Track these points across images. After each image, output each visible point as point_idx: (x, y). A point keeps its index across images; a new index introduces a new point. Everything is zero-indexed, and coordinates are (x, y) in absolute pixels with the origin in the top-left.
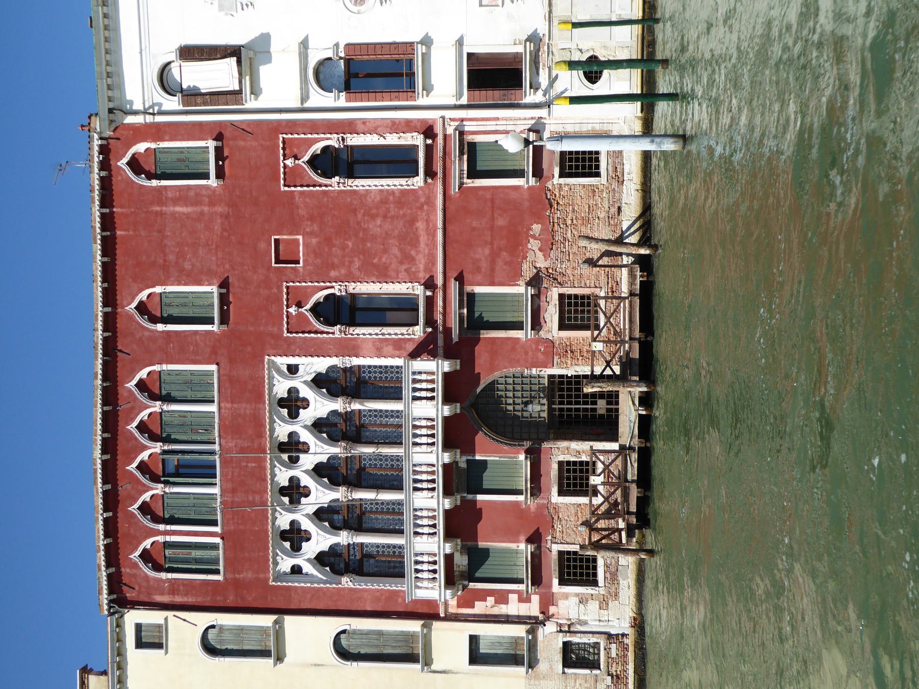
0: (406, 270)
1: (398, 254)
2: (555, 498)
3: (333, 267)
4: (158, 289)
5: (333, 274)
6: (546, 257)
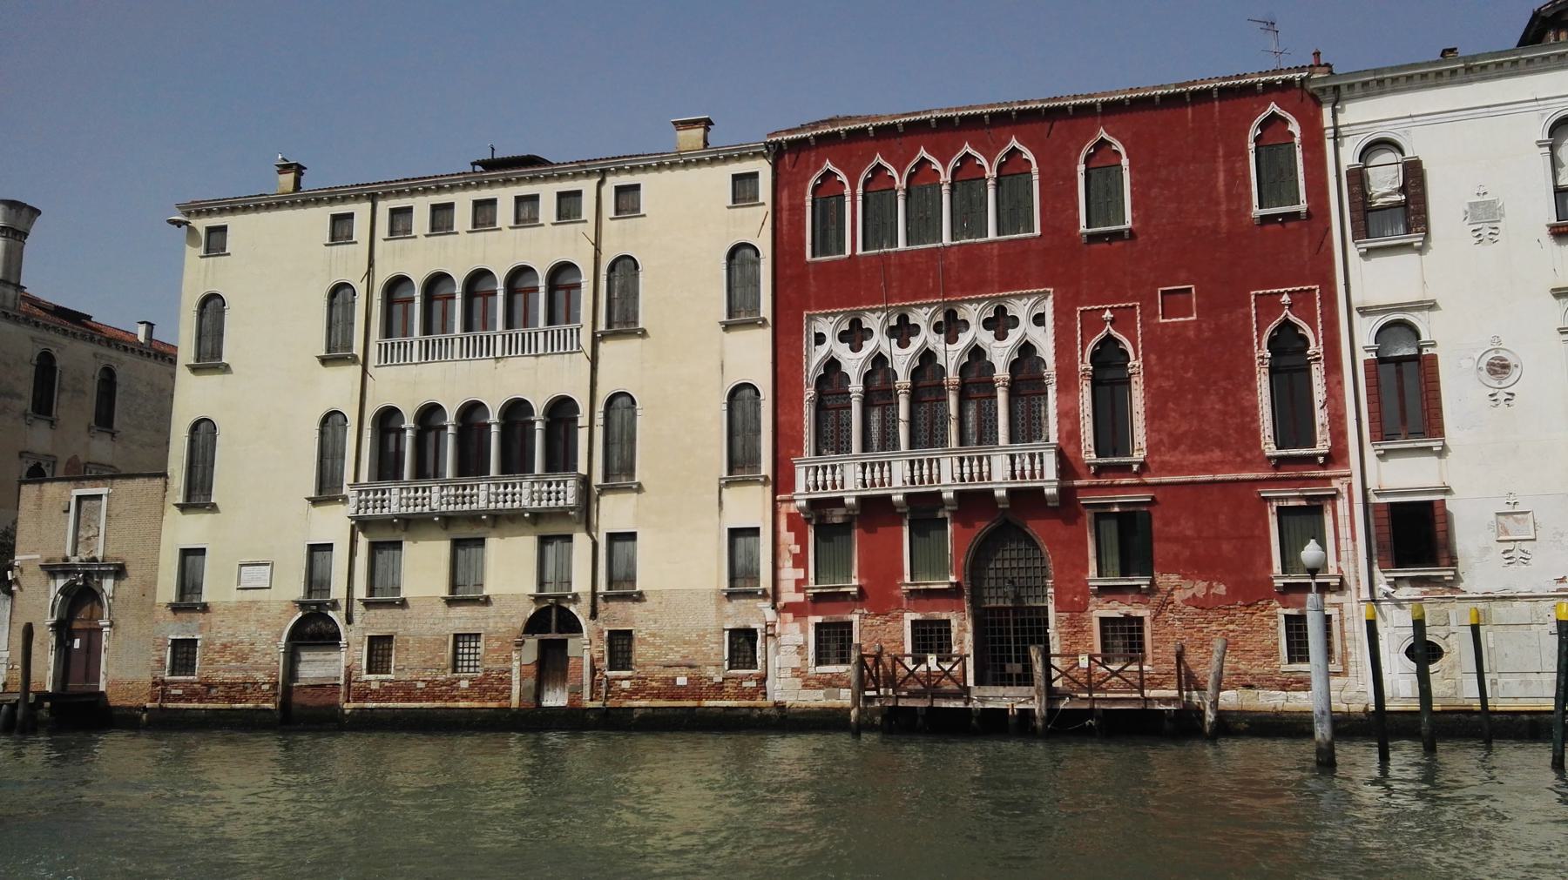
0: (1161, 441)
1: (1180, 431)
2: (909, 617)
3: (1161, 358)
4: (1125, 162)
5: (1153, 357)
6: (1187, 602)
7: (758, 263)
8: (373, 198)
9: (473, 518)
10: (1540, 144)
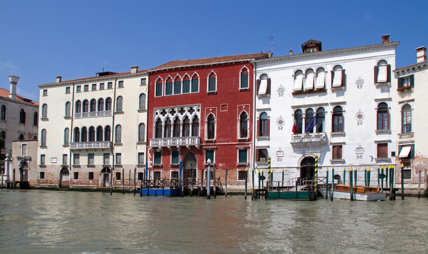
2: (171, 171)
4: (216, 77)
7: (145, 97)
8: (74, 84)
9: (92, 150)
10: (293, 76)
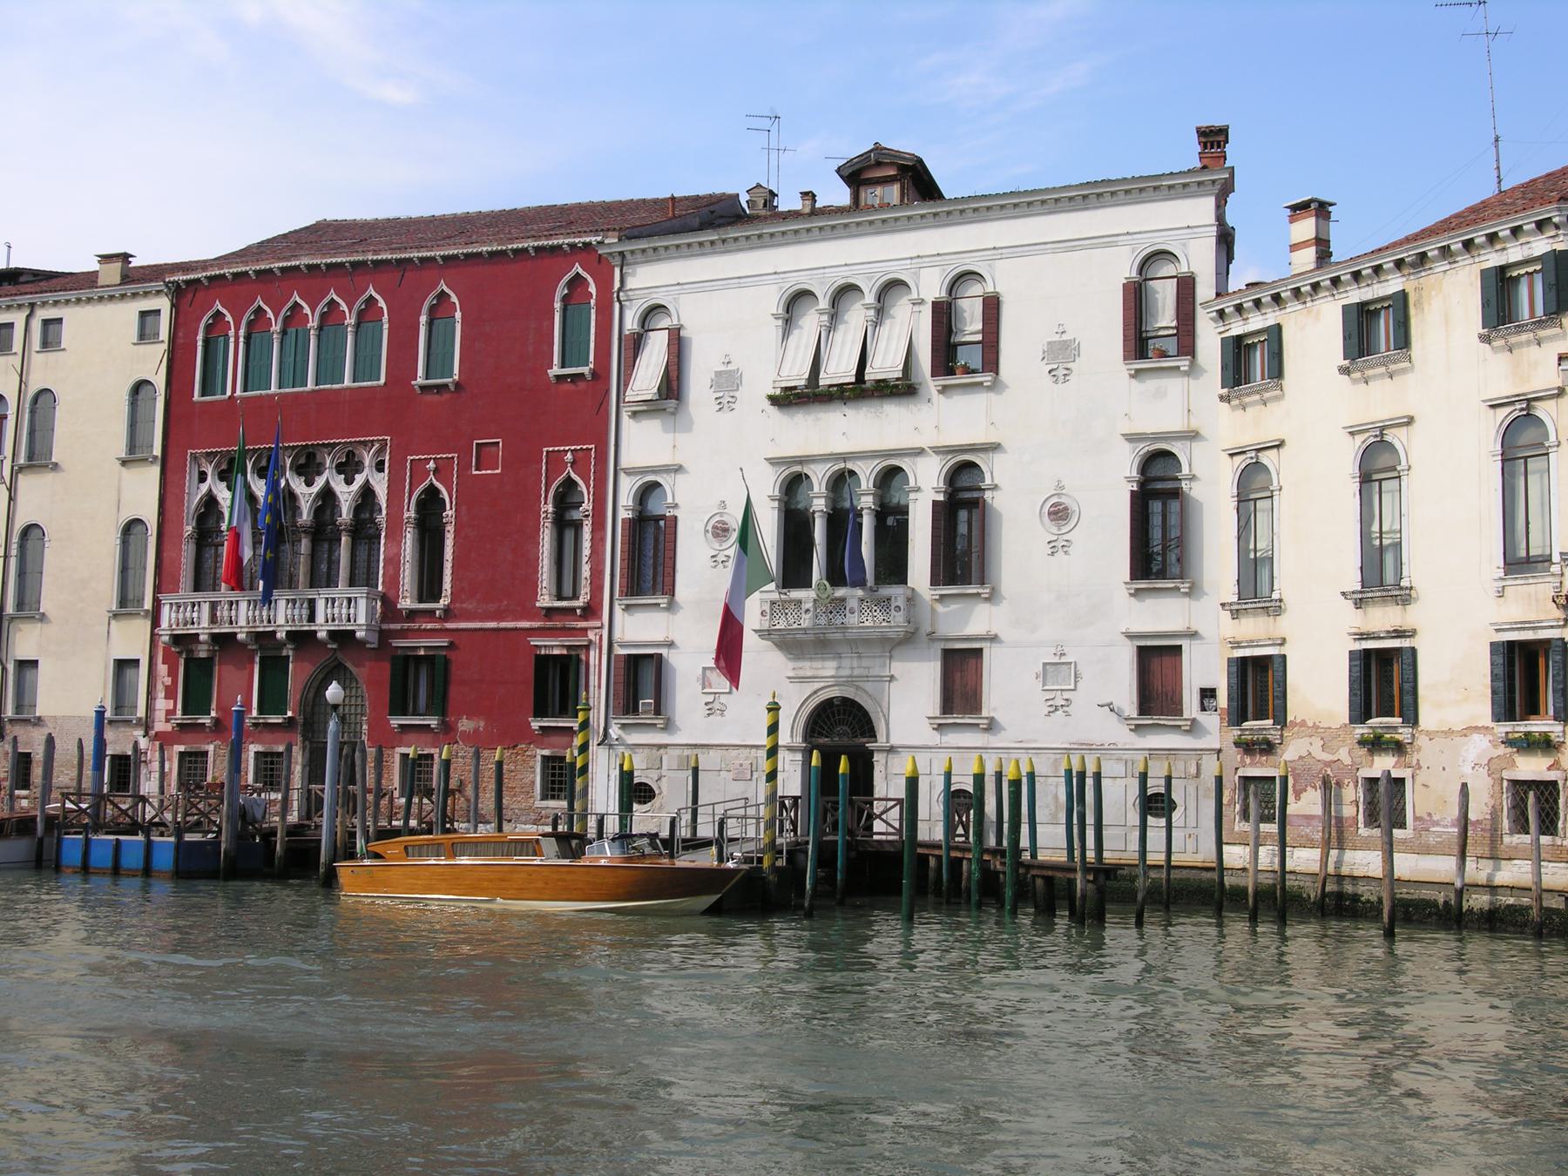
4: (458, 315)
5: (464, 508)
